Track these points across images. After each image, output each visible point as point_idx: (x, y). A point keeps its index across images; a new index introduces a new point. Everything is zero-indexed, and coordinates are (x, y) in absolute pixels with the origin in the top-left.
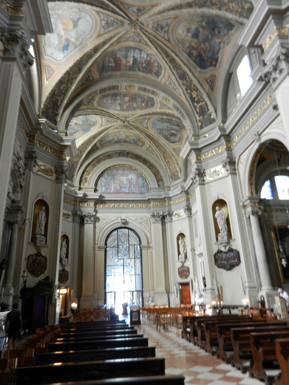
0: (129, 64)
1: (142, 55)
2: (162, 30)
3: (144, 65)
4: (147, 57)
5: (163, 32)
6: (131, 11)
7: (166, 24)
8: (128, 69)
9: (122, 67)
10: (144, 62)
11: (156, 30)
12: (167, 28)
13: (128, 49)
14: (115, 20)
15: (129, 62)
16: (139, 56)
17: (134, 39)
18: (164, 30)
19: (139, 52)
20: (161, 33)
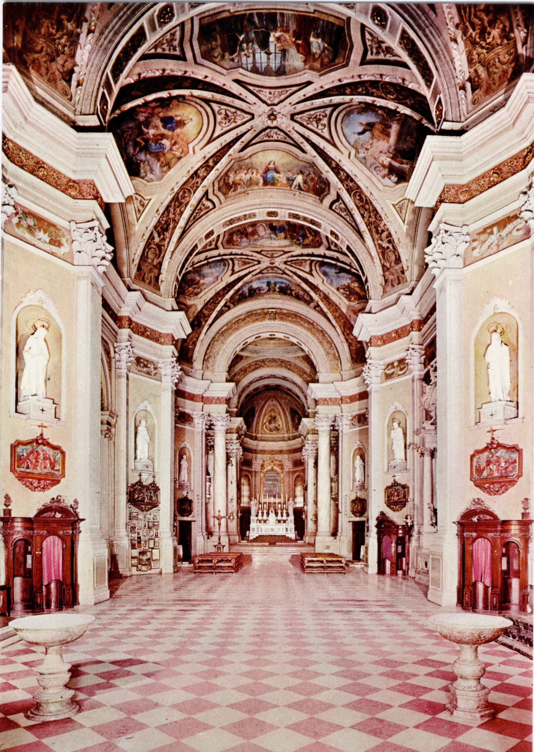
0: (278, 34)
1: (250, 60)
2: (227, 115)
3: (241, 38)
4: (240, 60)
5: (223, 112)
6: (282, 134)
7: (223, 125)
8: (278, 18)
9: (293, 26)
10: (245, 45)
11: (236, 112)
12: (219, 118)
13: (281, 72)
14: (305, 123)
15: (278, 39)
16: (257, 56)
17: (270, 93)
18: (223, 116)
19: (258, 65)
20: (226, 110)
